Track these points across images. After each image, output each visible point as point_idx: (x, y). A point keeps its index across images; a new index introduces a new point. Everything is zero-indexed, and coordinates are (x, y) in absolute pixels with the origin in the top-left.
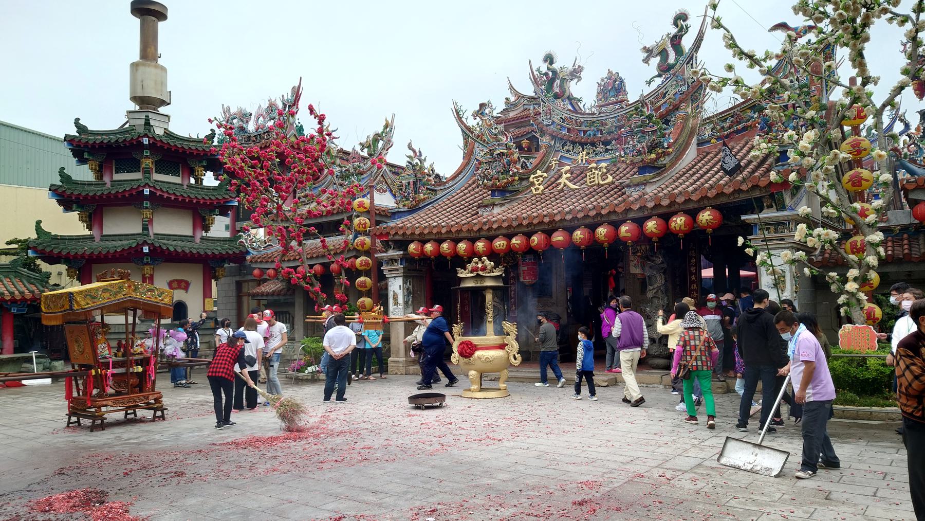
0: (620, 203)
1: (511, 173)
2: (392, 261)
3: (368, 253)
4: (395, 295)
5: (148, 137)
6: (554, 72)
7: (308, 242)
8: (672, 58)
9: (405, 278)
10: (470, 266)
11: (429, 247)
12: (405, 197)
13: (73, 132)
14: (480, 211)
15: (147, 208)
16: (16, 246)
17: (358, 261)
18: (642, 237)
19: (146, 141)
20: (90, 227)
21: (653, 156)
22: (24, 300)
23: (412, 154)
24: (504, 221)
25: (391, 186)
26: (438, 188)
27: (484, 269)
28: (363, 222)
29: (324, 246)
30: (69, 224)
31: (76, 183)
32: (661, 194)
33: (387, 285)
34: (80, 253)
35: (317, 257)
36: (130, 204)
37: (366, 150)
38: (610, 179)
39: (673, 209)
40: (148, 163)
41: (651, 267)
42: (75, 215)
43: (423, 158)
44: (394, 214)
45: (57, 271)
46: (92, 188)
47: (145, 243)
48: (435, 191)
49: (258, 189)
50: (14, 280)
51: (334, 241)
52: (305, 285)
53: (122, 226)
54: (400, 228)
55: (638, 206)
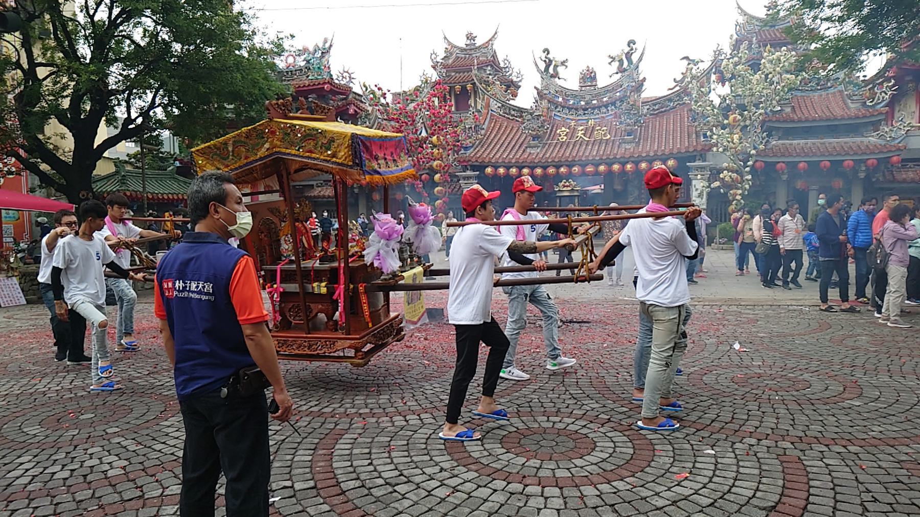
6: (551, 61)
8: (626, 63)
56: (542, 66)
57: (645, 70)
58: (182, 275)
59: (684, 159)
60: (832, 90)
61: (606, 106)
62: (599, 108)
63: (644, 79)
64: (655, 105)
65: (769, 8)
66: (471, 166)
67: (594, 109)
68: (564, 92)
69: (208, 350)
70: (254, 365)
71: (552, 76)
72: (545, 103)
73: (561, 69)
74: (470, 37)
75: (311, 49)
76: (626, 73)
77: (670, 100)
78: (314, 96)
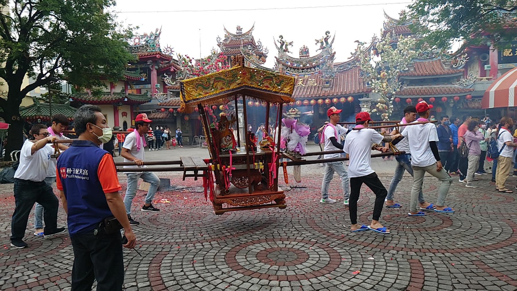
6: (284, 42)
56: (279, 45)
57: (335, 48)
58: (70, 166)
59: (358, 96)
60: (435, 59)
61: (314, 67)
62: (311, 68)
63: (335, 53)
64: (341, 67)
65: (401, 15)
67: (308, 69)
68: (291, 59)
69: (86, 208)
70: (113, 216)
71: (284, 51)
72: (280, 66)
73: (289, 47)
74: (239, 29)
75: (149, 35)
76: (325, 49)
77: (349, 64)
78: (151, 61)
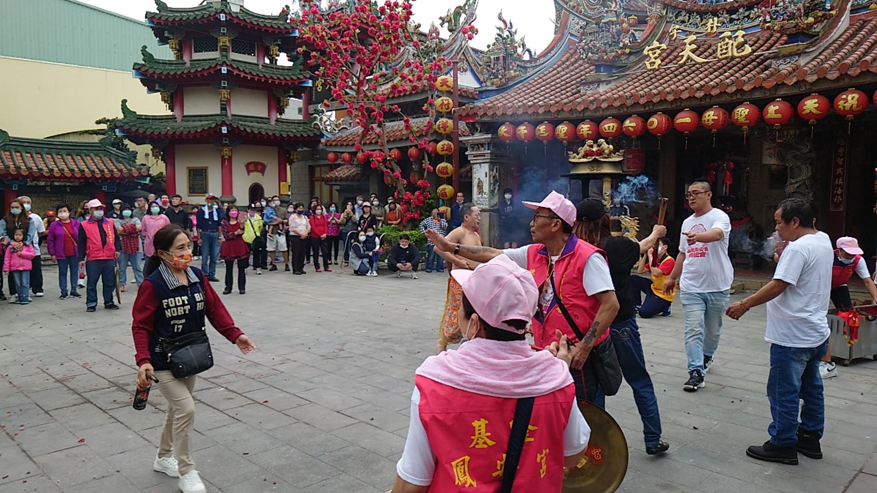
0: (768, 77)
1: (621, 45)
2: (478, 145)
3: (449, 137)
4: (480, 182)
5: (225, 13)
7: (387, 124)
9: (492, 164)
10: (582, 150)
11: (523, 130)
12: (493, 74)
13: (154, 9)
14: (582, 89)
15: (224, 88)
16: (104, 126)
17: (440, 145)
18: (795, 118)
19: (223, 17)
20: (172, 108)
21: (811, 20)
22: (113, 178)
23: (502, 25)
24: (615, 99)
25: (472, 65)
26: (528, 65)
27: (600, 153)
28: (446, 102)
29: (408, 127)
30: (152, 105)
31: (157, 62)
32: (826, 65)
33: (471, 169)
34: (163, 133)
35: (395, 141)
36: (208, 85)
37: (446, 25)
38: (748, 49)
39: (841, 83)
40: (224, 41)
41: (794, 157)
42: (158, 95)
43: (513, 30)
44: (482, 93)
45: (143, 151)
46: (173, 67)
47: (224, 123)
48: (525, 68)
49: (338, 62)
50: (103, 158)
51: (418, 123)
52: (385, 169)
53: (202, 107)
54: (490, 108)
55: (795, 80)
66: (483, 124)
